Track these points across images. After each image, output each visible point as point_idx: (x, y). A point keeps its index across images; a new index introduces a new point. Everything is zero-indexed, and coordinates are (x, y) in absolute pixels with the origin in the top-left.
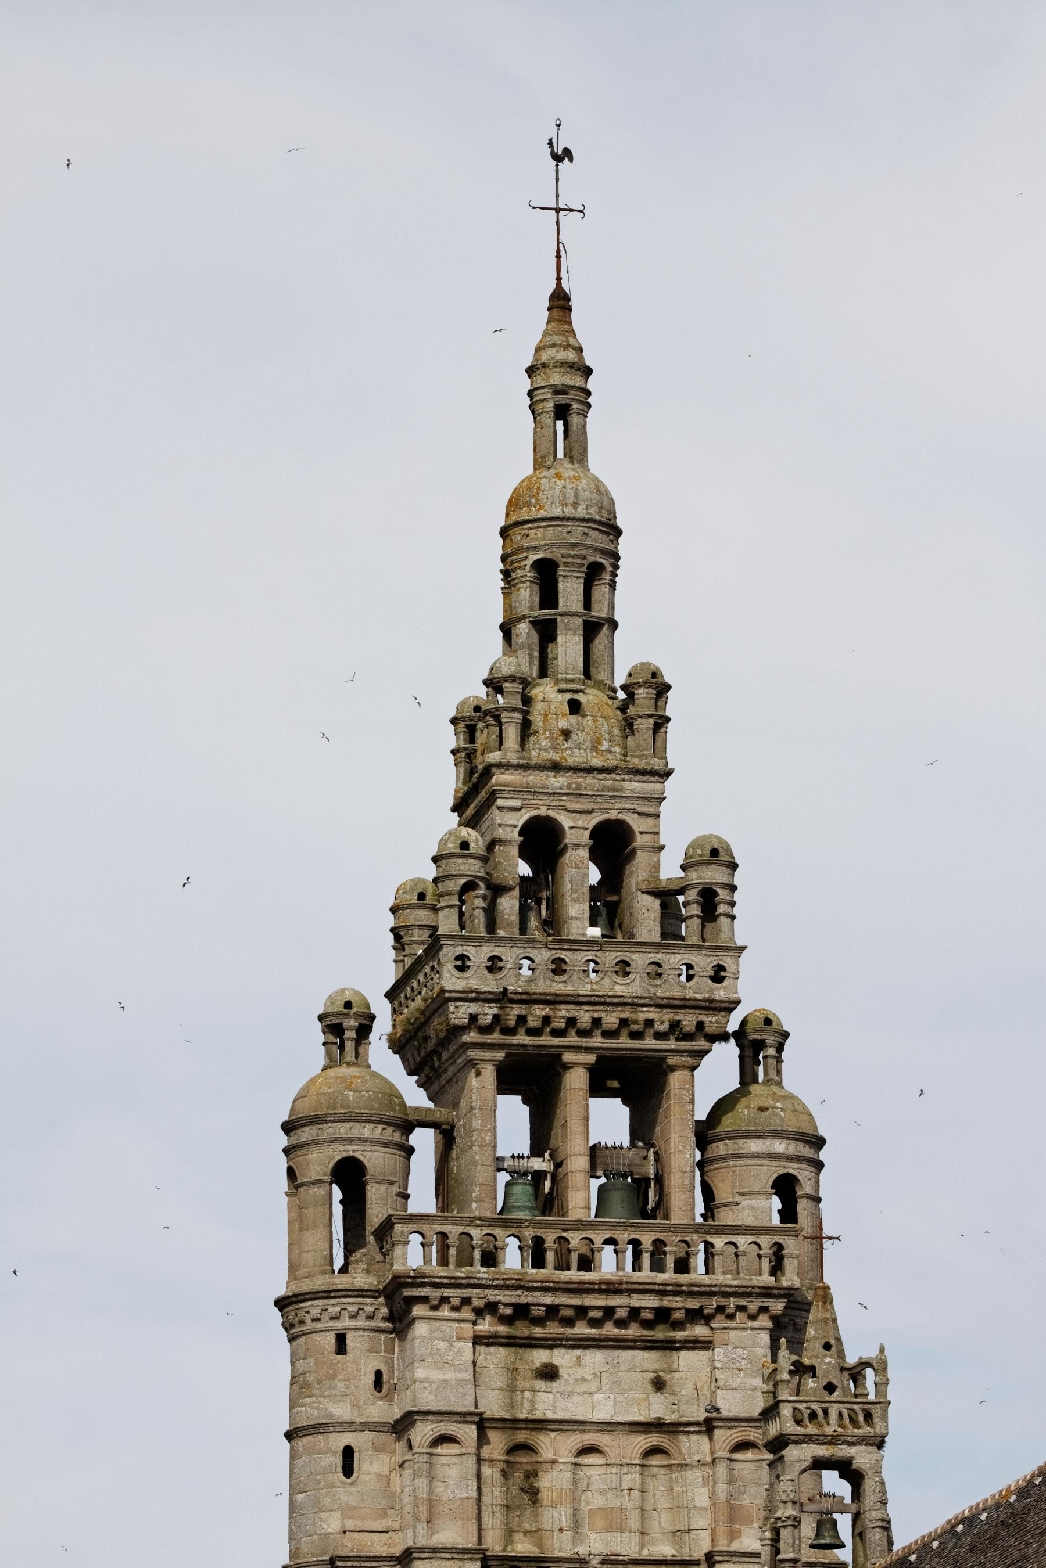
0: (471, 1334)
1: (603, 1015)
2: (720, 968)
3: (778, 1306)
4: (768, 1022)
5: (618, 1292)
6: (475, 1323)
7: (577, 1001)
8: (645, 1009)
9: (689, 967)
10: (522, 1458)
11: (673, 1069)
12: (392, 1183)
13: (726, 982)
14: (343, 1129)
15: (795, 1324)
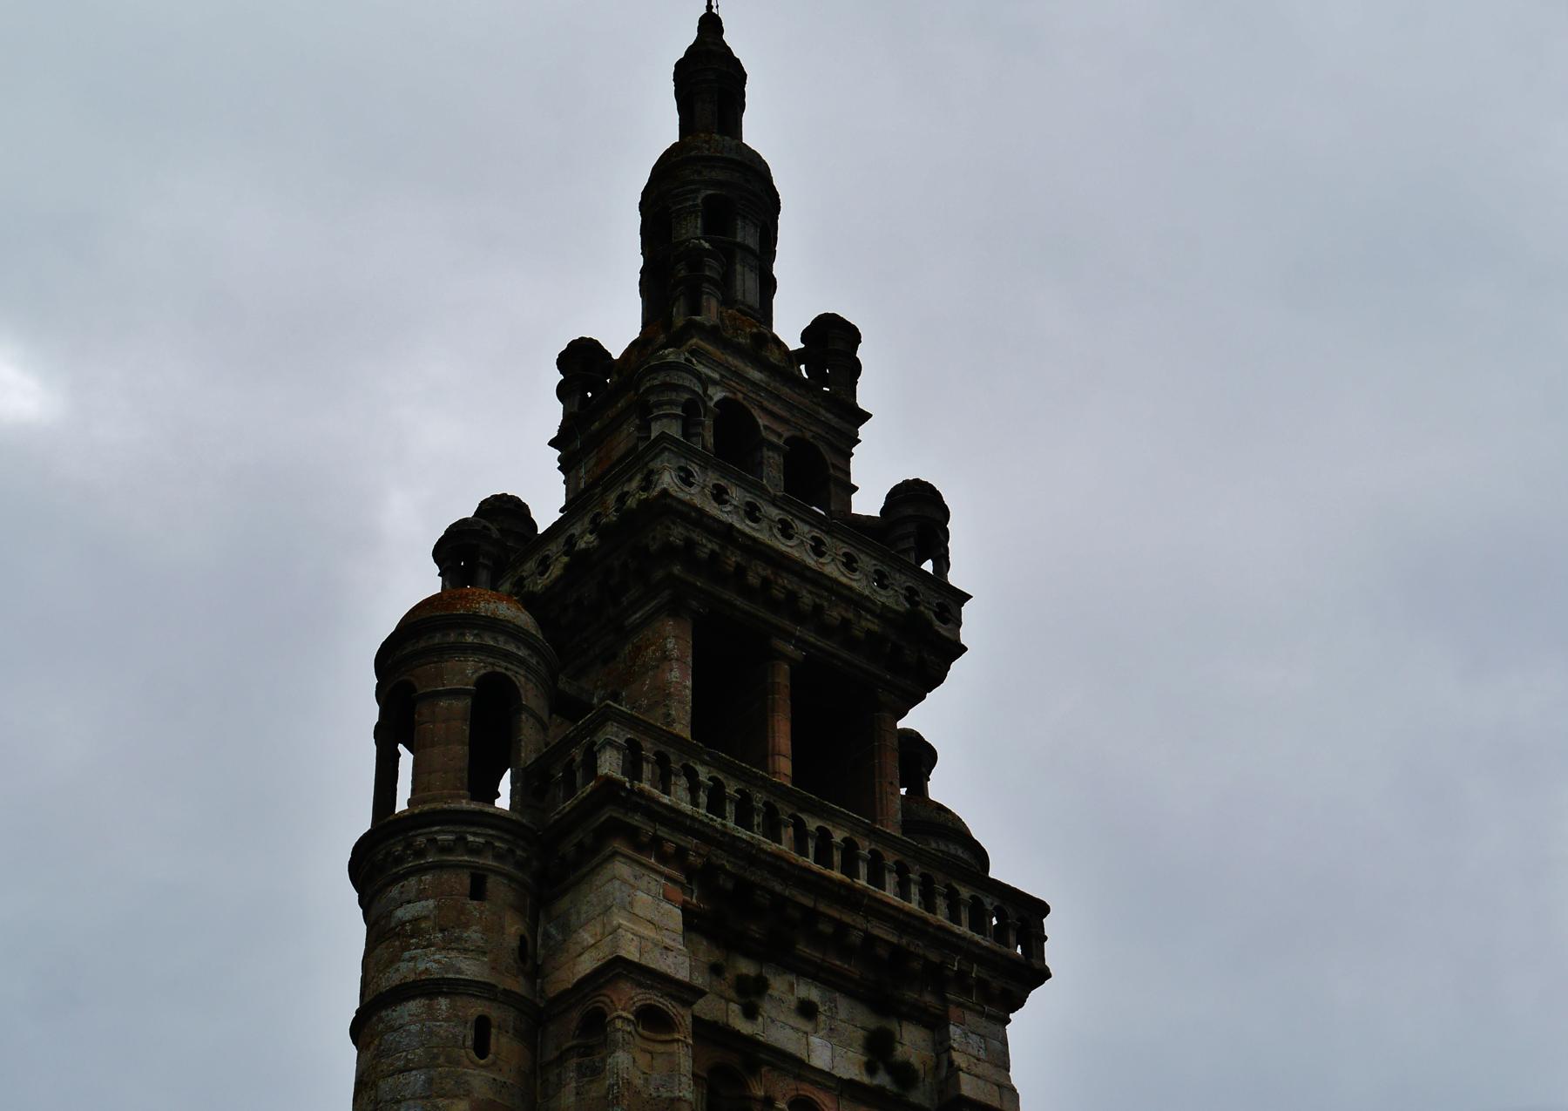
1: (825, 604)
8: (869, 617)
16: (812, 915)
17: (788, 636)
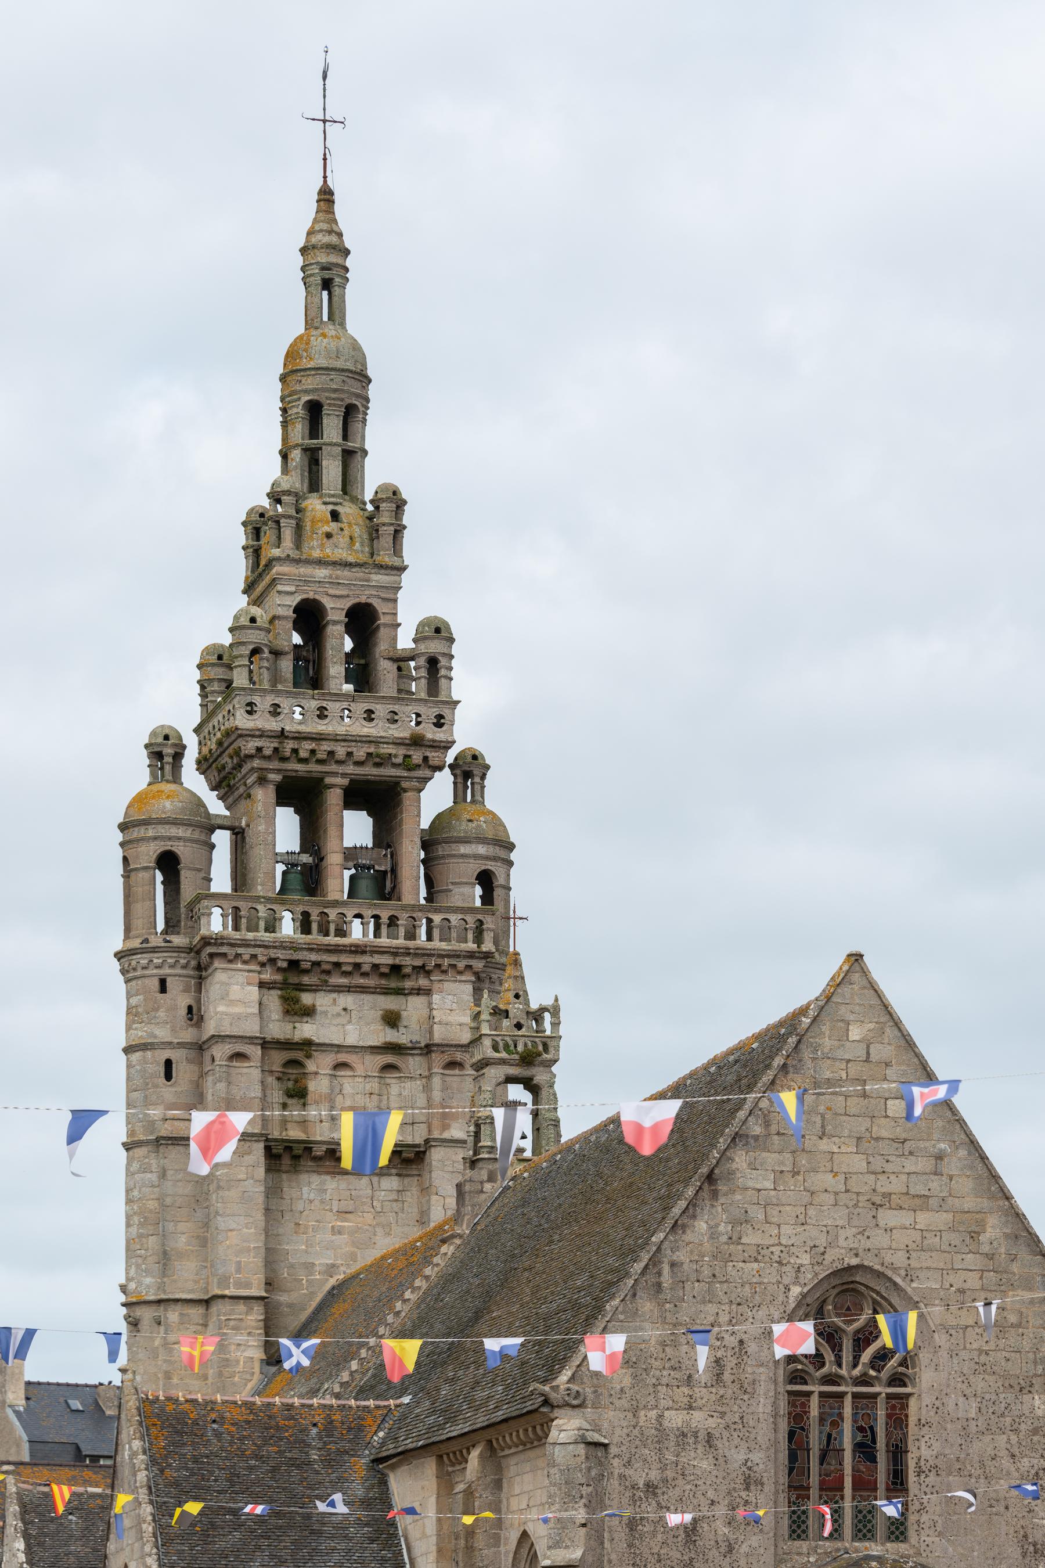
0: (258, 981)
1: (354, 750)
2: (440, 717)
3: (478, 965)
4: (475, 757)
5: (364, 952)
6: (259, 973)
7: (335, 739)
8: (385, 746)
9: (418, 715)
10: (293, 1071)
11: (405, 790)
12: (199, 870)
13: (444, 728)
14: (163, 830)
15: (490, 978)
16: (337, 965)
17: (335, 774)
